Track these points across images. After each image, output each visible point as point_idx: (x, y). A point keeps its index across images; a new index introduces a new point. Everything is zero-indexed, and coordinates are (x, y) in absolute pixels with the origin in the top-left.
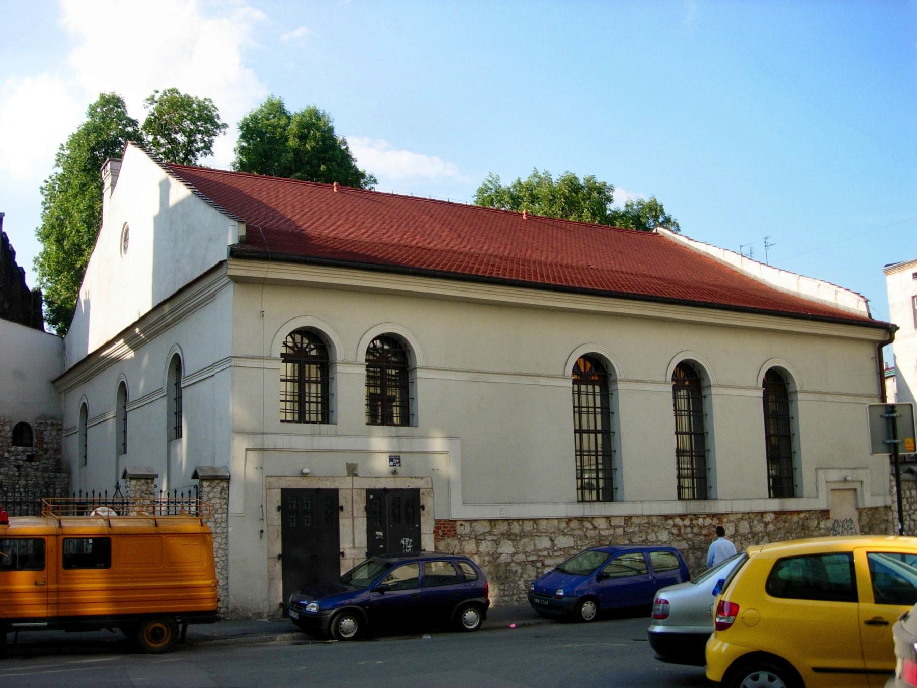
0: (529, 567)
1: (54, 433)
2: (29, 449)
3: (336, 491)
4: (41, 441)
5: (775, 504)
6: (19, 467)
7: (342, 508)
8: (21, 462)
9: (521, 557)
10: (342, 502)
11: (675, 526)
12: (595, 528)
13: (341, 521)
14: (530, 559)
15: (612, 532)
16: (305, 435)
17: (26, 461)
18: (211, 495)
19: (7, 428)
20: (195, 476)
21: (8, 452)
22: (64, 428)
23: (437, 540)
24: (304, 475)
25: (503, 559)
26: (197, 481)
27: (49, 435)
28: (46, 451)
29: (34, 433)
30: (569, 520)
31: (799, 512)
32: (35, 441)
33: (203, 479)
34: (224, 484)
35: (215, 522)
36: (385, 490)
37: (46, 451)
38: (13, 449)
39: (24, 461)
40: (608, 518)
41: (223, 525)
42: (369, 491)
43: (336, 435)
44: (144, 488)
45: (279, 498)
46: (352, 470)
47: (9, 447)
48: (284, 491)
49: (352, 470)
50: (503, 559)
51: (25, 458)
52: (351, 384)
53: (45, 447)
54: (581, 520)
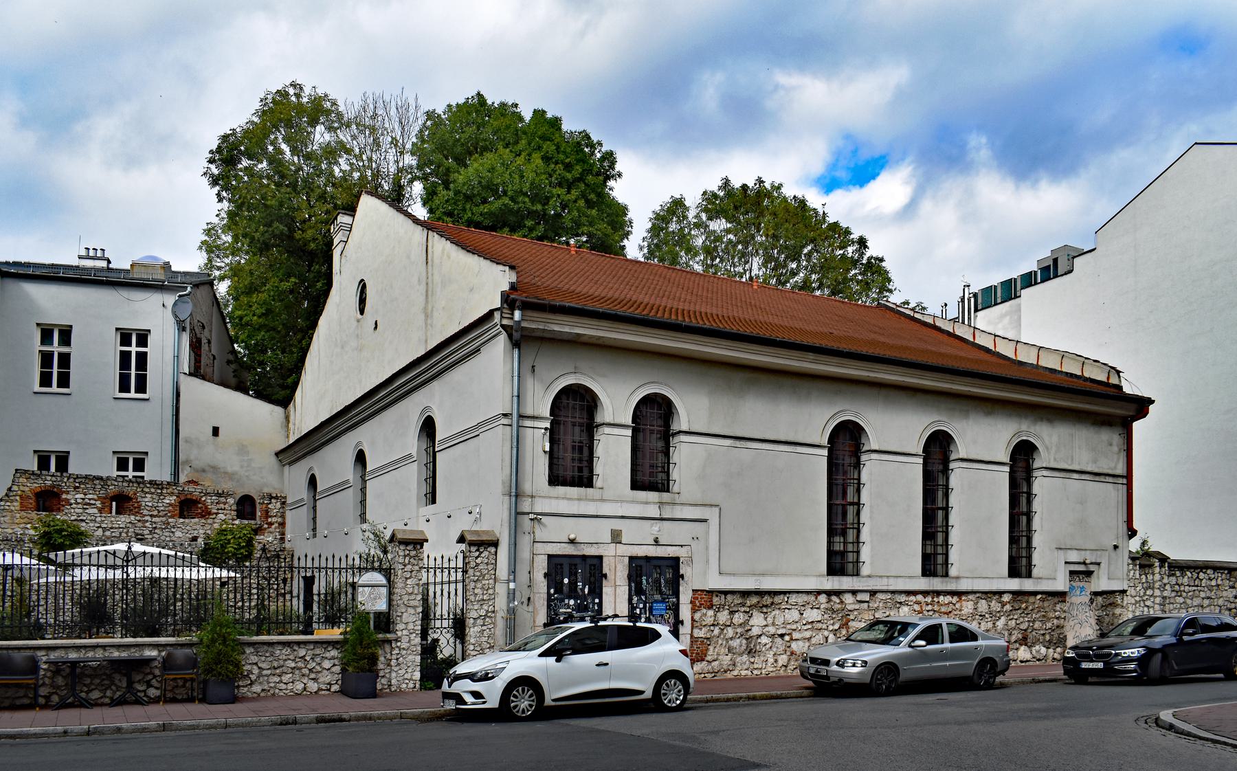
0: (779, 640)
3: (600, 558)
4: (267, 514)
5: (1015, 584)
7: (605, 576)
9: (772, 630)
10: (606, 570)
11: (918, 603)
12: (842, 602)
13: (604, 590)
14: (780, 632)
15: (857, 606)
18: (479, 561)
19: (231, 501)
20: (461, 540)
23: (694, 611)
25: (755, 631)
26: (463, 546)
27: (275, 506)
28: (271, 524)
29: (258, 507)
30: (819, 593)
31: (1035, 593)
32: (259, 514)
33: (471, 544)
34: (493, 550)
35: (482, 588)
36: (647, 559)
37: (271, 524)
40: (854, 592)
41: (491, 591)
42: (631, 558)
44: (413, 553)
45: (545, 564)
46: (616, 537)
49: (616, 537)
50: (755, 631)
52: (613, 452)
54: (829, 593)
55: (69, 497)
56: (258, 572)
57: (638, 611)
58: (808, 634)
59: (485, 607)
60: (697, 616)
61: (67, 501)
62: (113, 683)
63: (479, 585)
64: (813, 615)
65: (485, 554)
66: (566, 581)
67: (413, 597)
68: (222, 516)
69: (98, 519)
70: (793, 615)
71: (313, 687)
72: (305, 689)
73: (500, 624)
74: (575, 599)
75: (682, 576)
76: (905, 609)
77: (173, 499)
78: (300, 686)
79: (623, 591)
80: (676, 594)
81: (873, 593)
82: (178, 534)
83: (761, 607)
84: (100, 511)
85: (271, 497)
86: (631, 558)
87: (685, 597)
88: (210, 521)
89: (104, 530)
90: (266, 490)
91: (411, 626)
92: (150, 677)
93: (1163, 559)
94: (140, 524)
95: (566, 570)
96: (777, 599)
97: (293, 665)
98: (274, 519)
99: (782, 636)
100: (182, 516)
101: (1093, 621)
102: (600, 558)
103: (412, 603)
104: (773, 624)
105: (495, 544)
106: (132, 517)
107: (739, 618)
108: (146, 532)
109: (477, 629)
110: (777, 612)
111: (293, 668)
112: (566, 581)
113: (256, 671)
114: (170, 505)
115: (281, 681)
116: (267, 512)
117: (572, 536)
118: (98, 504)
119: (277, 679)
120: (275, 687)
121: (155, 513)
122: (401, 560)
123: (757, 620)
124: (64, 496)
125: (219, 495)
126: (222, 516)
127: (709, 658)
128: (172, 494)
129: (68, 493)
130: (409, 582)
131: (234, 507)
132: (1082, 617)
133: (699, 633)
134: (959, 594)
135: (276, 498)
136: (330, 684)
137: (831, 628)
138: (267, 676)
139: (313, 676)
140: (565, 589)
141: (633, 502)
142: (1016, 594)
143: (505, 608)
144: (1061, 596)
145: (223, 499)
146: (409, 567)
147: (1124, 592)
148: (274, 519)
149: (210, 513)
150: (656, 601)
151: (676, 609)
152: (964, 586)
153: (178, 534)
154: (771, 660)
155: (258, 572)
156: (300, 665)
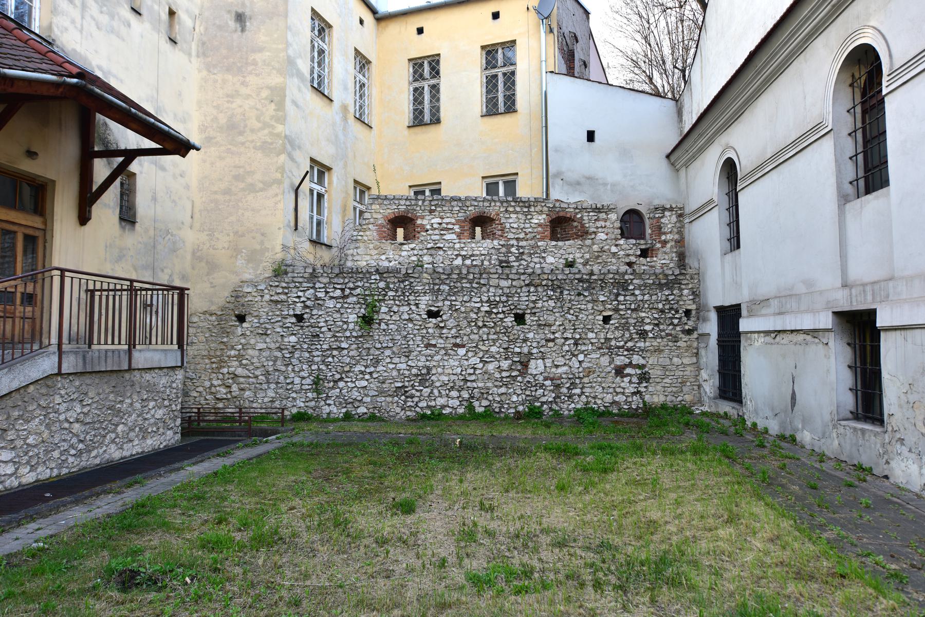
1: (674, 219)
2: (642, 242)
4: (659, 230)
6: (630, 264)
8: (633, 259)
17: (640, 256)
19: (613, 216)
21: (616, 245)
22: (687, 211)
27: (669, 220)
28: (665, 243)
29: (647, 223)
32: (648, 231)
37: (665, 243)
38: (622, 242)
39: (637, 256)
47: (616, 239)
51: (639, 253)
53: (663, 237)
55: (425, 222)
61: (422, 226)
68: (602, 236)
69: (457, 246)
77: (540, 219)
84: (459, 236)
85: (664, 209)
88: (588, 242)
89: (464, 258)
90: (657, 202)
94: (504, 250)
98: (669, 237)
100: (554, 237)
106: (496, 242)
108: (512, 258)
114: (540, 225)
116: (660, 228)
118: (457, 228)
121: (522, 236)
124: (419, 222)
125: (598, 210)
126: (602, 236)
129: (423, 218)
131: (618, 224)
135: (671, 209)
145: (603, 216)
148: (669, 237)
149: (587, 233)
153: (550, 259)
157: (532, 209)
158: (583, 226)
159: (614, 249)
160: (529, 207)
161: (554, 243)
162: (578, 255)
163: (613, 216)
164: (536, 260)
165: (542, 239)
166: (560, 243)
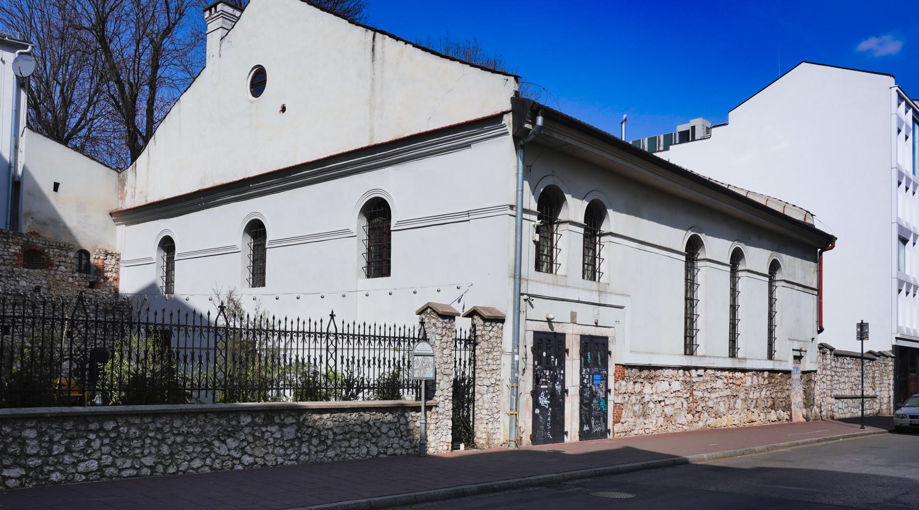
3: (564, 335)
9: (655, 397)
16: (548, 284)
17: (89, 287)
18: (491, 334)
19: (72, 254)
23: (616, 381)
24: (549, 321)
25: (647, 398)
34: (500, 325)
38: (77, 275)
39: (86, 287)
40: (697, 368)
41: (498, 362)
42: (583, 337)
43: (566, 286)
47: (73, 273)
48: (536, 333)
50: (647, 398)
56: (327, 338)
57: (585, 381)
58: (673, 401)
59: (494, 376)
60: (617, 384)
62: (212, 451)
63: (491, 357)
64: (676, 386)
65: (495, 329)
66: (544, 354)
67: (447, 366)
70: (664, 386)
71: (374, 450)
72: (368, 453)
73: (506, 392)
74: (550, 369)
75: (610, 353)
76: (720, 381)
78: (364, 451)
79: (577, 363)
80: (606, 366)
81: (705, 369)
82: (23, 283)
83: (650, 379)
86: (582, 337)
87: (611, 370)
88: (52, 272)
91: (446, 393)
92: (245, 444)
93: (832, 349)
95: (545, 342)
96: (658, 372)
97: (359, 430)
99: (660, 402)
101: (802, 392)
102: (564, 335)
103: (448, 372)
104: (656, 393)
105: (502, 321)
107: (638, 387)
109: (490, 395)
110: (658, 383)
111: (359, 433)
112: (544, 354)
113: (331, 437)
114: (15, 254)
115: (350, 446)
117: (551, 316)
119: (347, 444)
120: (345, 452)
122: (439, 331)
123: (648, 389)
126: (63, 268)
127: (622, 420)
128: (18, 244)
130: (445, 352)
132: (797, 389)
133: (619, 400)
134: (744, 371)
136: (386, 447)
137: (685, 396)
138: (340, 441)
139: (374, 440)
140: (544, 361)
141: (584, 289)
142: (772, 372)
143: (509, 377)
144: (788, 373)
145: (64, 253)
146: (445, 338)
147: (815, 371)
149: (52, 265)
150: (596, 373)
151: (605, 378)
152: (748, 365)
154: (654, 422)
155: (327, 338)
156: (365, 429)
157: (10, 240)
158: (49, 259)
159: (70, 280)
160: (8, 238)
161: (26, 270)
162: (44, 282)
163: (72, 254)
164: (13, 282)
165: (17, 266)
166: (31, 271)
